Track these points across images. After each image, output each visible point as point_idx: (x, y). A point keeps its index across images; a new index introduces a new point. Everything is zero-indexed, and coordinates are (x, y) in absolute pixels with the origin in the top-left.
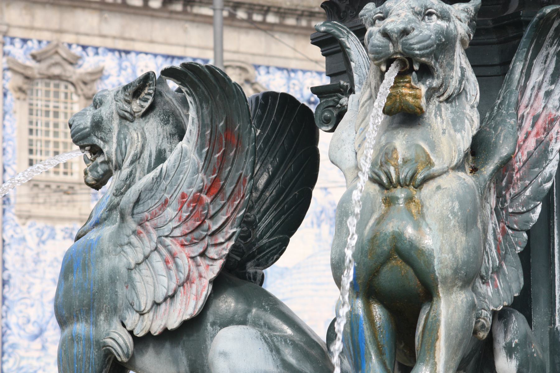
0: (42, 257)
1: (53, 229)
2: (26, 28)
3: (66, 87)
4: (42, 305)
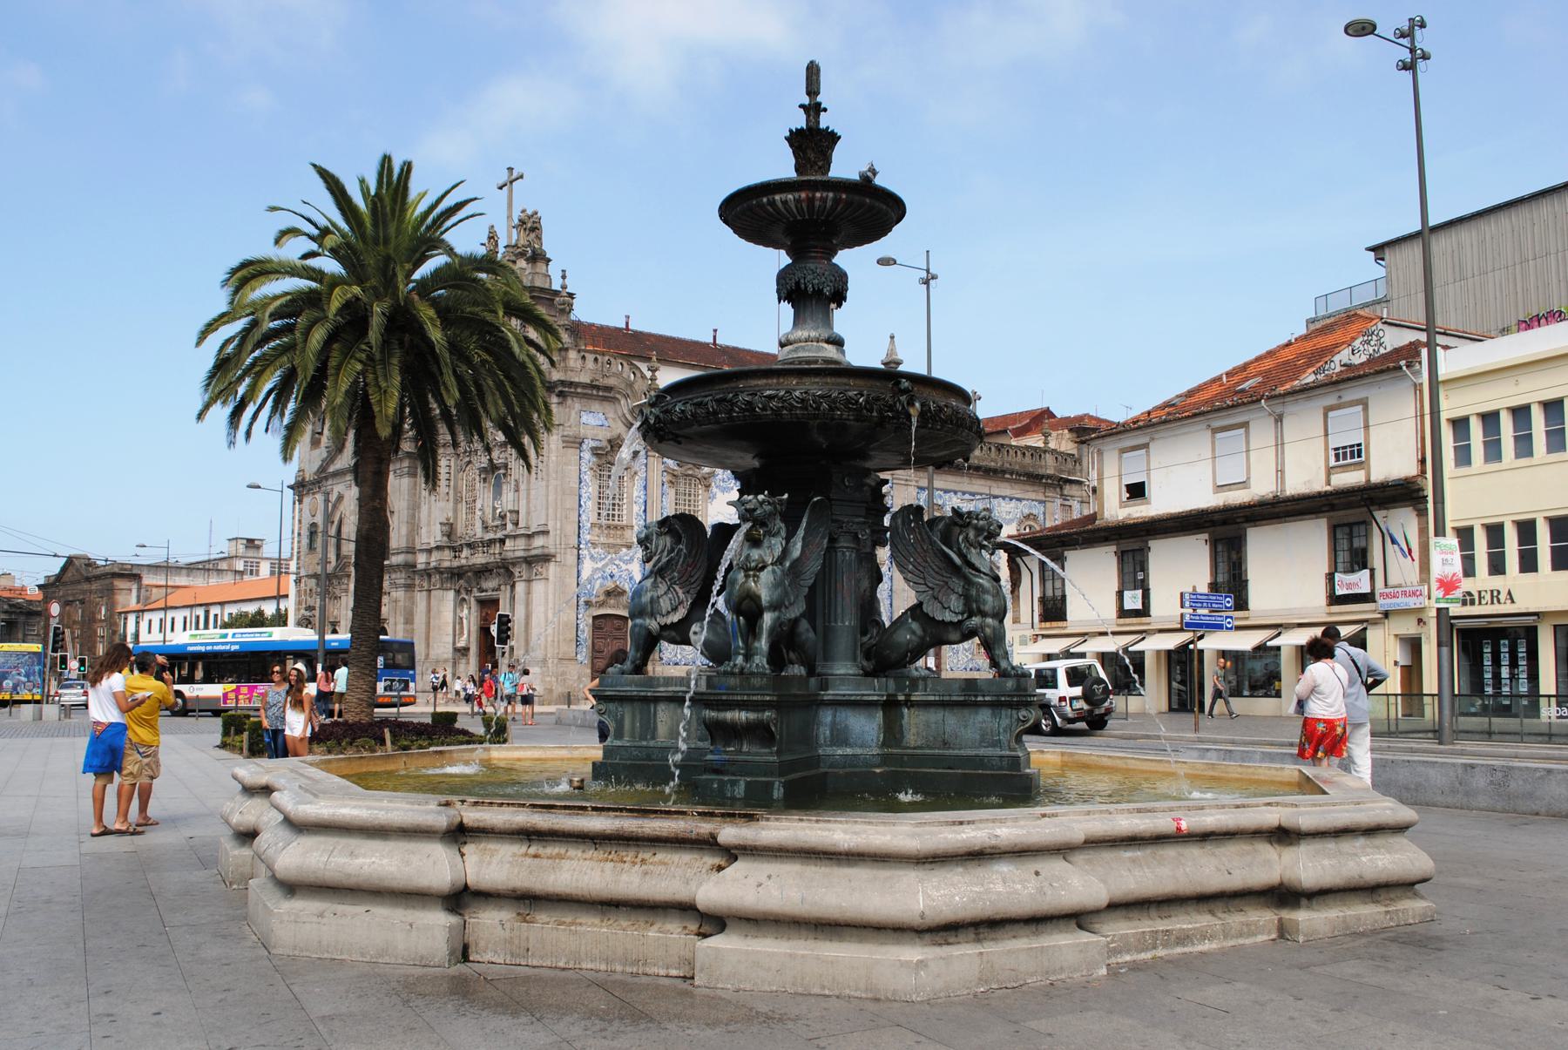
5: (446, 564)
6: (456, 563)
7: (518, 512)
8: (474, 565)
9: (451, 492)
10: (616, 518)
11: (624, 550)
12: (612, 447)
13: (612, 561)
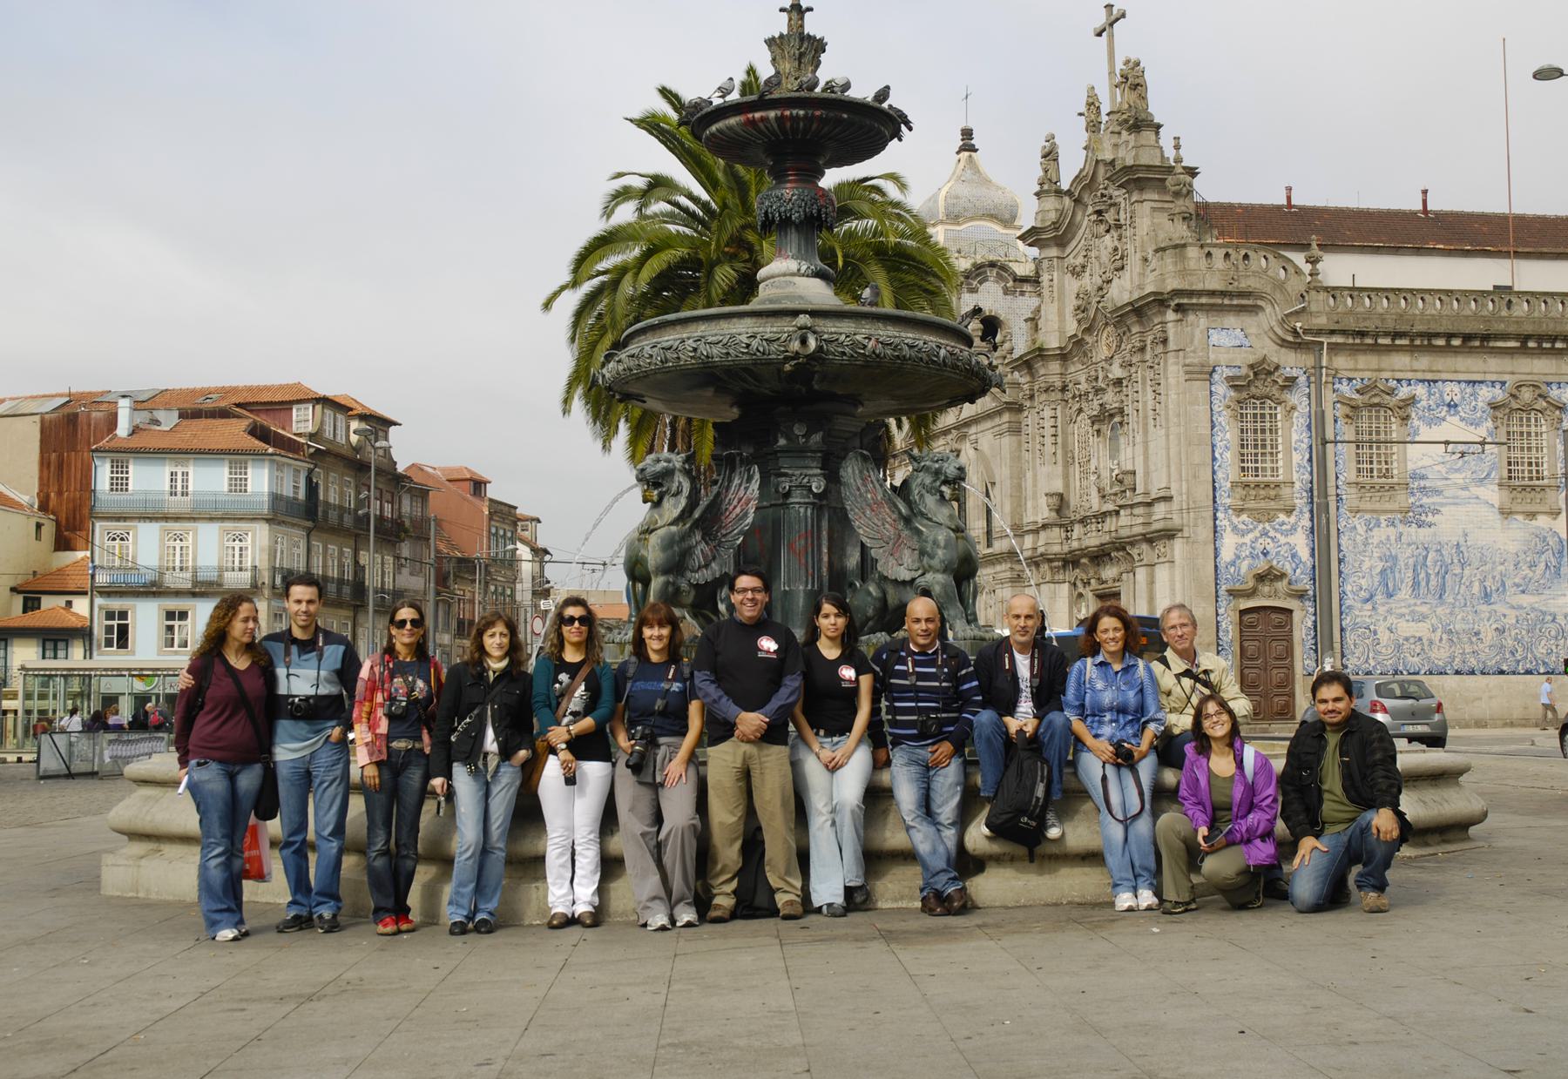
0: (1370, 541)
1: (1378, 520)
2: (1350, 370)
3: (1385, 412)
4: (1372, 576)
5: (1056, 549)
6: (1066, 549)
7: (1134, 473)
8: (1087, 548)
9: (1059, 452)
10: (1269, 473)
11: (1282, 517)
12: (1256, 374)
13: (1265, 534)
